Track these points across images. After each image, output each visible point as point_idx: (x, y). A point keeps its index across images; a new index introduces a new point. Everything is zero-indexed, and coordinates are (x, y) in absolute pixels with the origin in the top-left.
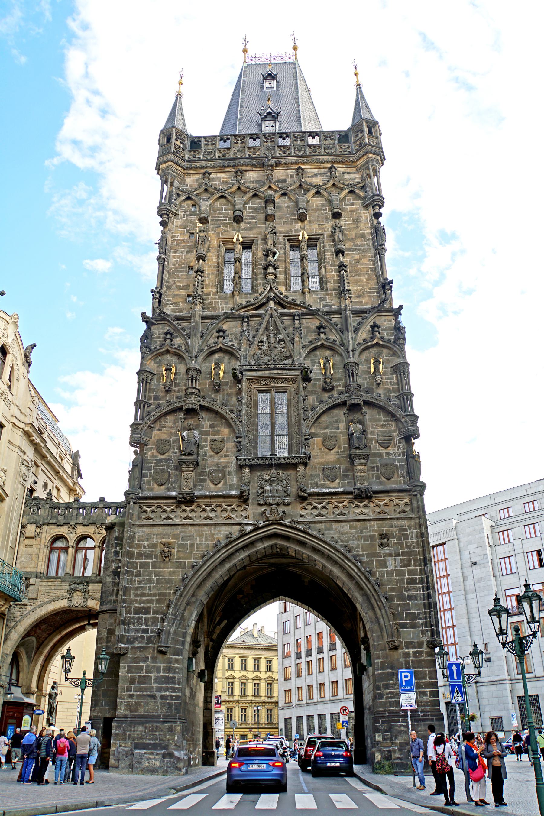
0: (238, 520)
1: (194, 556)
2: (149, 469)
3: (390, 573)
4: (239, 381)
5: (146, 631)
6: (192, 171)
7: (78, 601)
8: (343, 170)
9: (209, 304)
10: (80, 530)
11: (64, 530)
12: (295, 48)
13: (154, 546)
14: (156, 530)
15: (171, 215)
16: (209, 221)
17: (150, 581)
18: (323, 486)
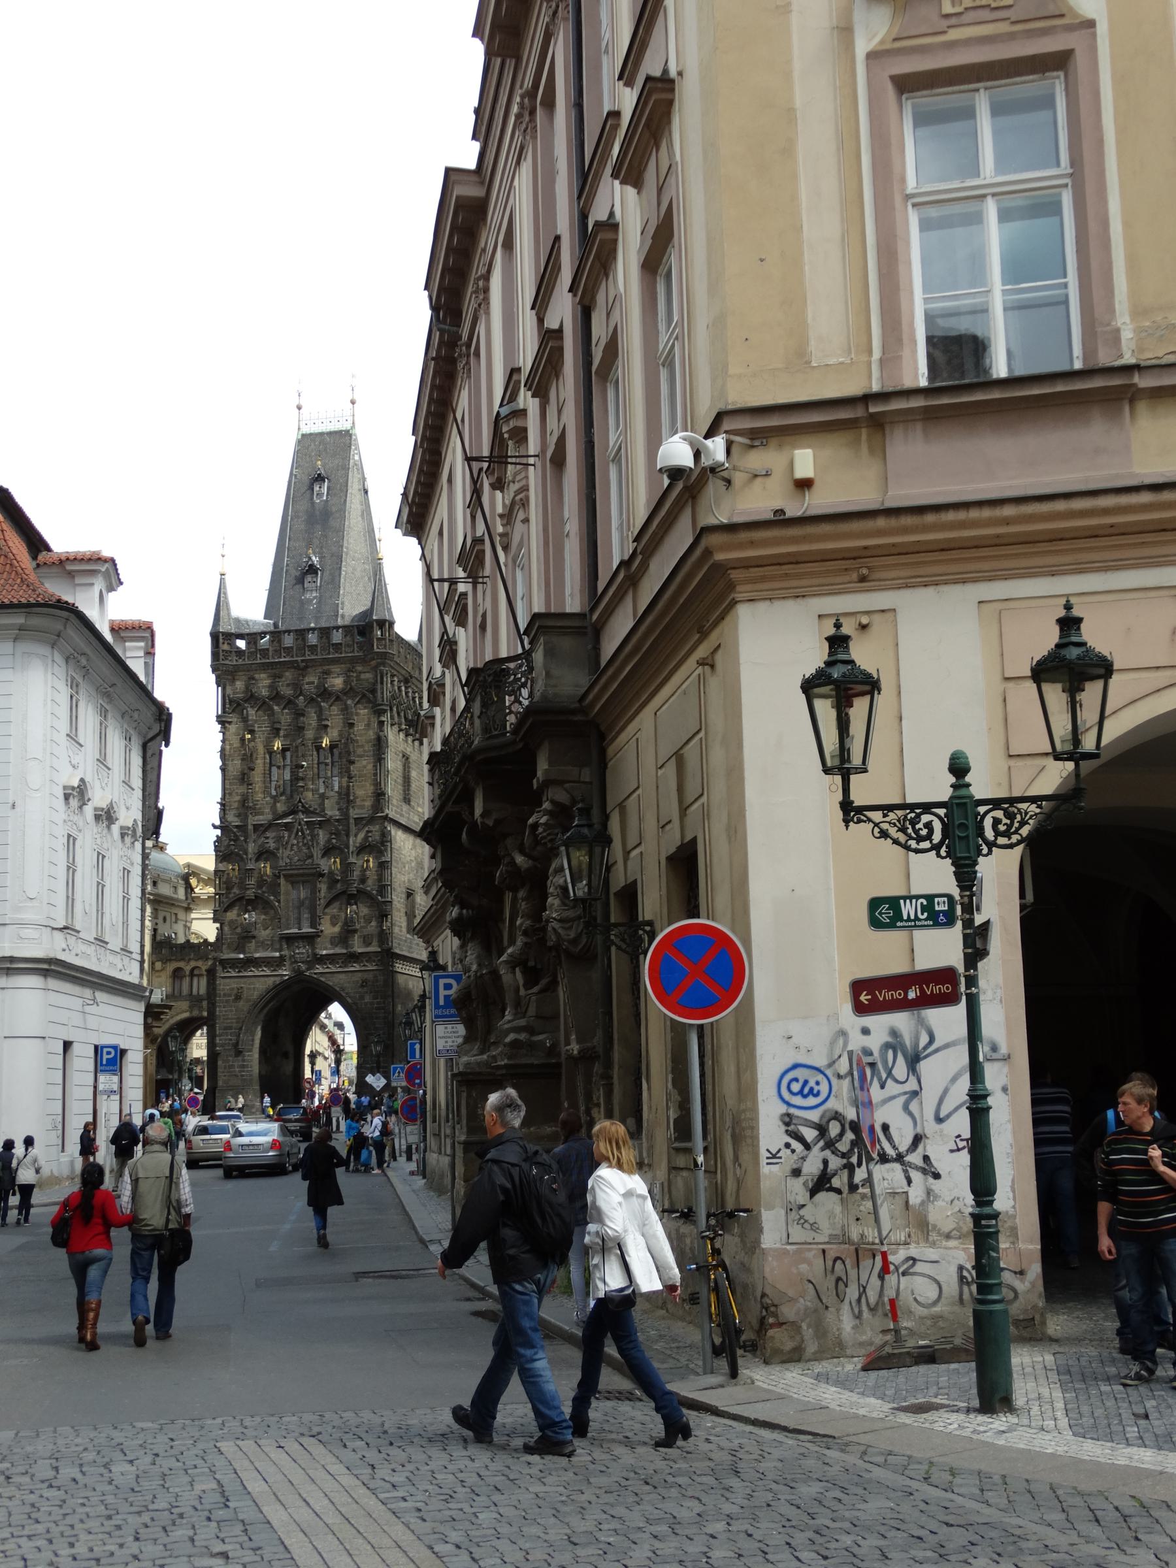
0: (280, 972)
1: (256, 995)
2: (226, 939)
3: (366, 1004)
4: (279, 877)
5: (231, 1040)
6: (240, 673)
7: (196, 1013)
8: (359, 668)
9: (260, 809)
10: (193, 964)
11: (181, 964)
12: (353, 402)
13: (233, 989)
14: (232, 980)
15: (227, 725)
16: (256, 729)
17: (231, 1011)
18: (330, 949)
